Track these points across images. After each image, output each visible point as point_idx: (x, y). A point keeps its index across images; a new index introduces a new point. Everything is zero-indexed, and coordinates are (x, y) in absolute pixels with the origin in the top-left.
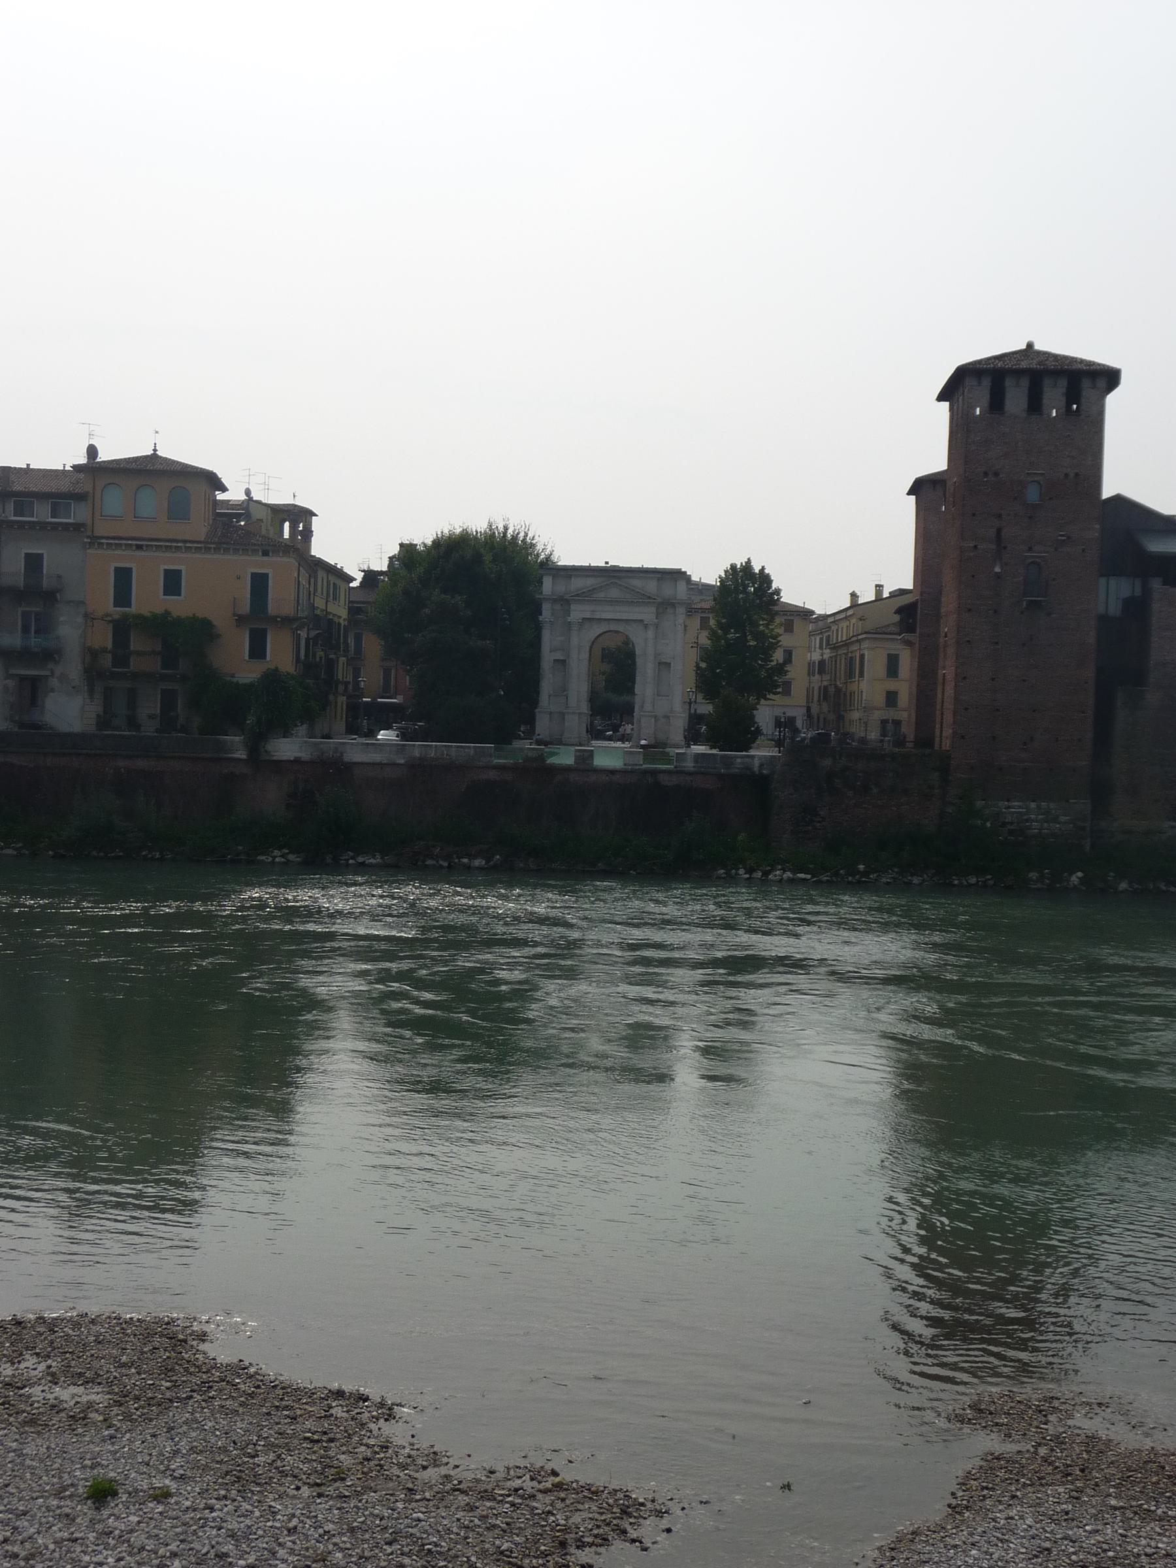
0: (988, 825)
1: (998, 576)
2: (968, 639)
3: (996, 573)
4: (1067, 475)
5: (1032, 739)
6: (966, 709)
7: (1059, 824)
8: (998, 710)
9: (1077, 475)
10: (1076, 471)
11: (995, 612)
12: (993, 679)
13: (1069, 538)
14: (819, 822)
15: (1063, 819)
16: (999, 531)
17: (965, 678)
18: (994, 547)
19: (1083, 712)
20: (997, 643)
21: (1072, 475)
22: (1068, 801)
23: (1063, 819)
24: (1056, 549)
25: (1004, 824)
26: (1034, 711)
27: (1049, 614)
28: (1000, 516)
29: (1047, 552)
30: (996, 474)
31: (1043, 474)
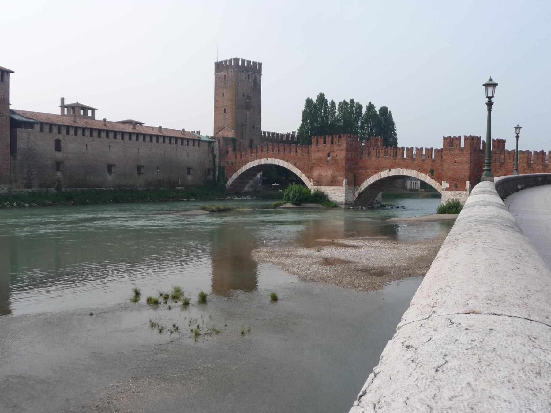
4: (1, 98)
9: (4, 98)
10: (4, 97)
13: (3, 114)
15: (6, 189)
21: (3, 98)
22: (6, 184)
23: (6, 189)
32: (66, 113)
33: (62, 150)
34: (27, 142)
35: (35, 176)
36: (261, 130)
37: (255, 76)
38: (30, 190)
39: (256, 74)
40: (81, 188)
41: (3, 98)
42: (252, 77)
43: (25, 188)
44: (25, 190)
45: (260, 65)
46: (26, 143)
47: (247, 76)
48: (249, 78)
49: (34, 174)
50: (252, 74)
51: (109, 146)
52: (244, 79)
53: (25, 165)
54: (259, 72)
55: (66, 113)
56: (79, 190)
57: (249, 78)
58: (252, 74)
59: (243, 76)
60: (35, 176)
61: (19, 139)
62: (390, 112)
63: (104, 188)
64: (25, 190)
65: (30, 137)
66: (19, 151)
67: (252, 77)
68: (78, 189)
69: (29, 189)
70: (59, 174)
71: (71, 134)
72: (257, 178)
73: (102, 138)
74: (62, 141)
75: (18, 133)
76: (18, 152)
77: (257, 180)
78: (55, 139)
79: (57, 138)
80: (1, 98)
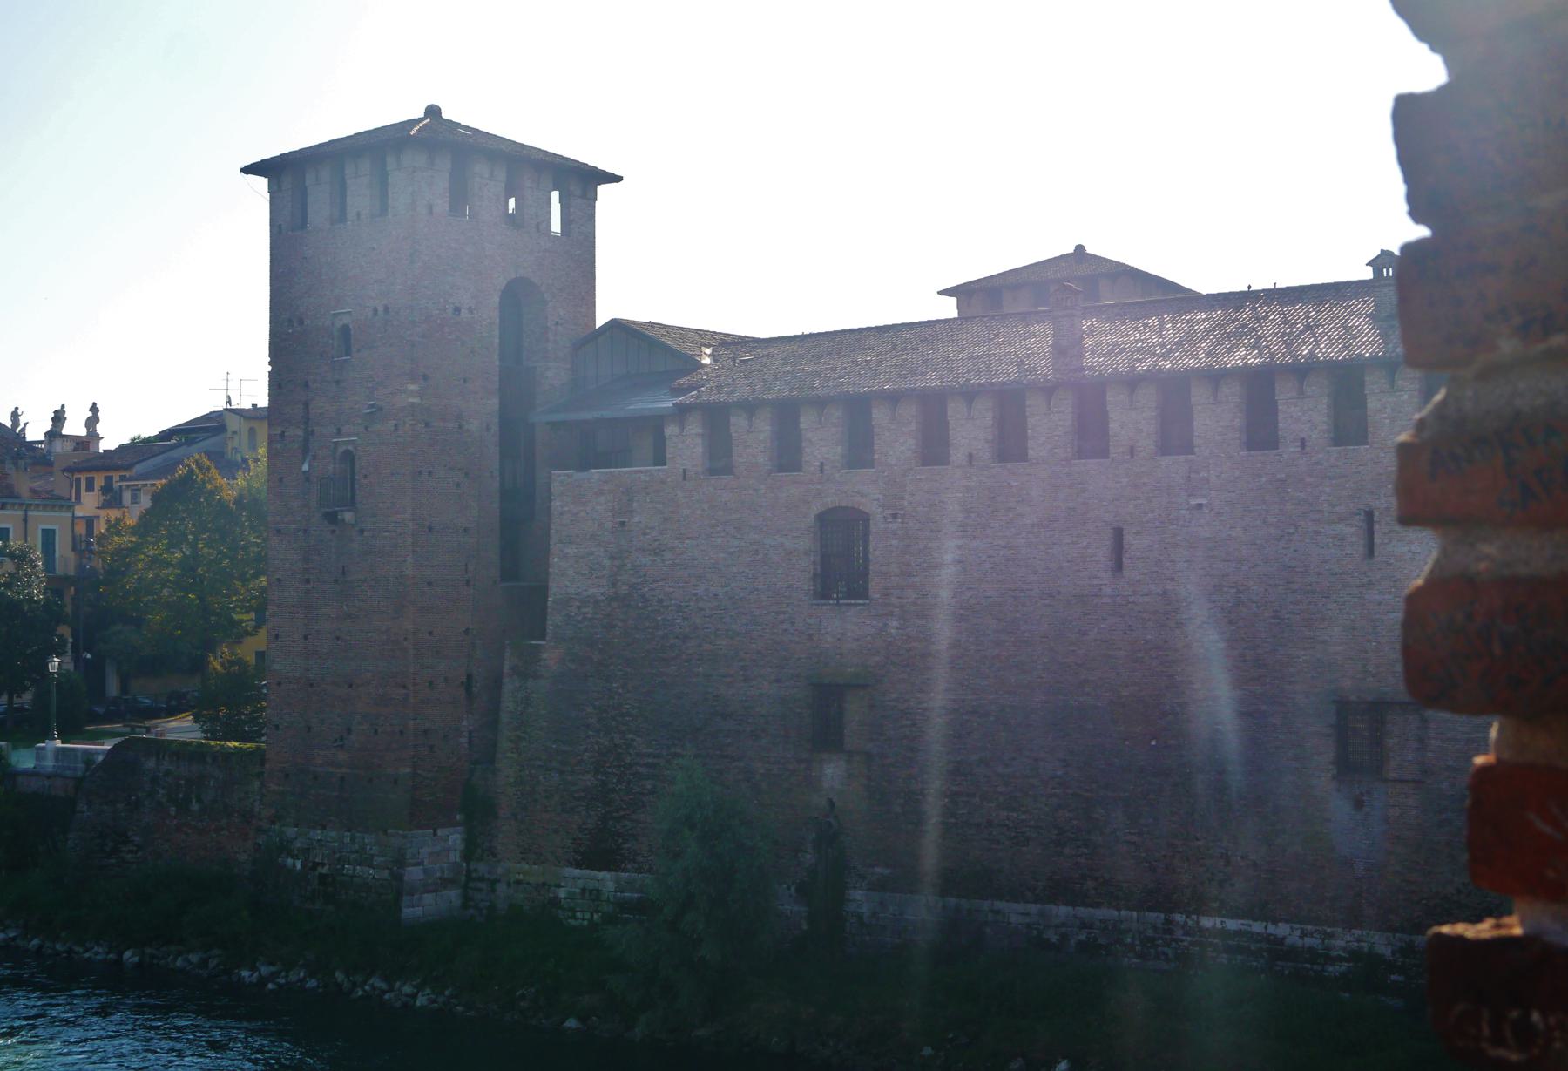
0: (298, 866)
1: (307, 477)
2: (278, 576)
3: (304, 472)
4: (375, 311)
5: (349, 731)
6: (279, 684)
7: (374, 868)
8: (311, 685)
9: (386, 309)
11: (305, 531)
12: (306, 638)
13: (380, 409)
14: (131, 852)
16: (306, 405)
17: (277, 636)
18: (300, 433)
19: (404, 687)
20: (308, 581)
21: (380, 310)
24: (366, 428)
25: (316, 865)
26: (350, 686)
27: (362, 531)
28: (306, 385)
29: (357, 435)
30: (301, 322)
31: (350, 312)
32: (1385, 270)
33: (875, 586)
34: (613, 558)
35: (649, 785)
38: (606, 880)
40: (1034, 908)
41: (380, 310)
43: (579, 865)
44: (573, 880)
46: (607, 562)
49: (641, 770)
51: (1369, 515)
53: (590, 709)
55: (1385, 270)
56: (1014, 919)
60: (649, 785)
61: (560, 541)
63: (1282, 930)
64: (573, 880)
65: (636, 519)
66: (554, 619)
68: (999, 905)
69: (601, 875)
70: (832, 772)
71: (958, 456)
73: (1294, 448)
74: (877, 526)
75: (556, 504)
76: (550, 628)
78: (816, 509)
79: (832, 500)
80: (375, 311)
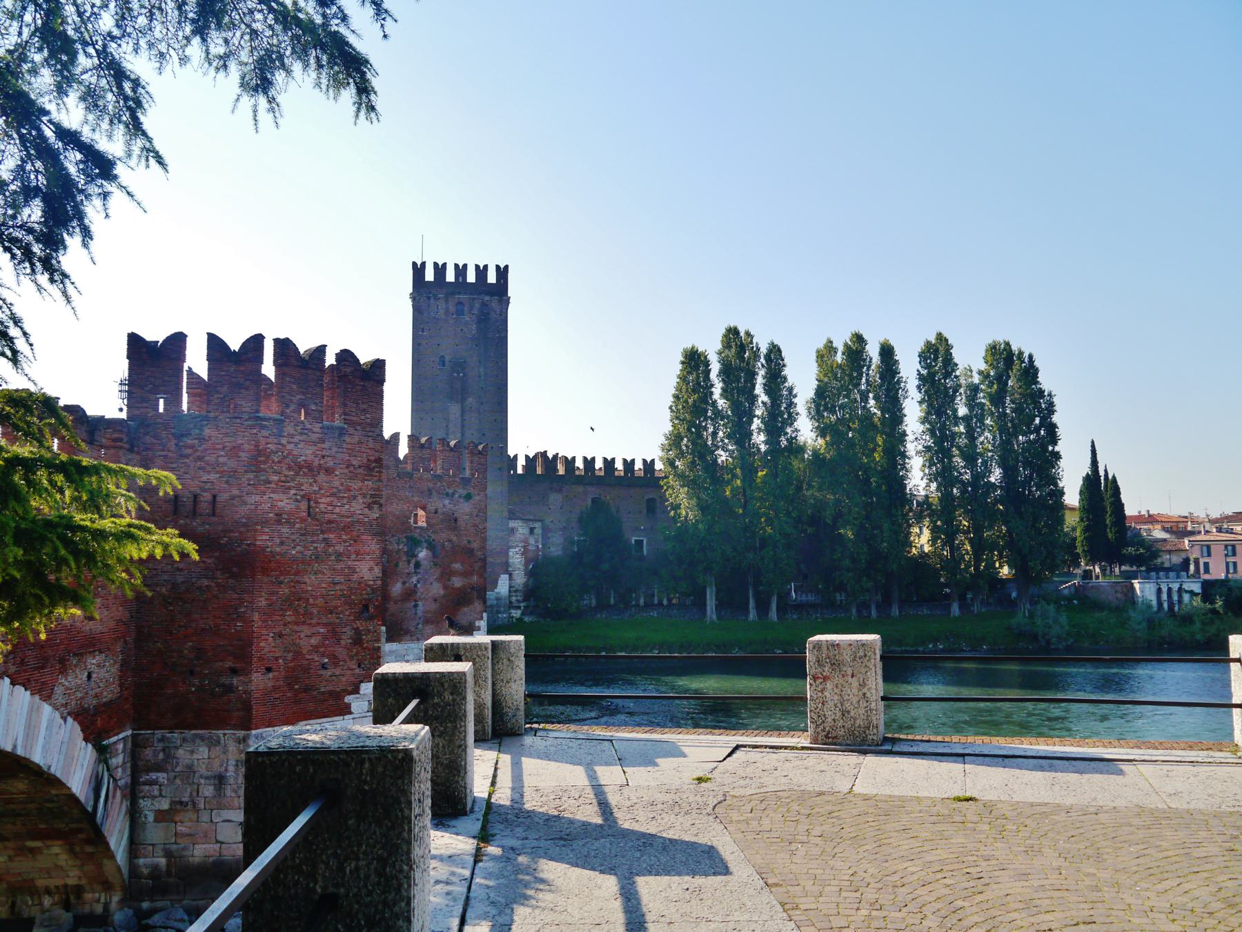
36: (511, 453)
37: (484, 304)
39: (487, 298)
42: (471, 309)
45: (503, 273)
47: (452, 308)
48: (460, 313)
50: (474, 299)
52: (443, 317)
54: (500, 290)
57: (460, 313)
58: (474, 299)
59: (440, 307)
62: (1031, 357)
67: (471, 309)
72: (498, 593)
77: (498, 599)
